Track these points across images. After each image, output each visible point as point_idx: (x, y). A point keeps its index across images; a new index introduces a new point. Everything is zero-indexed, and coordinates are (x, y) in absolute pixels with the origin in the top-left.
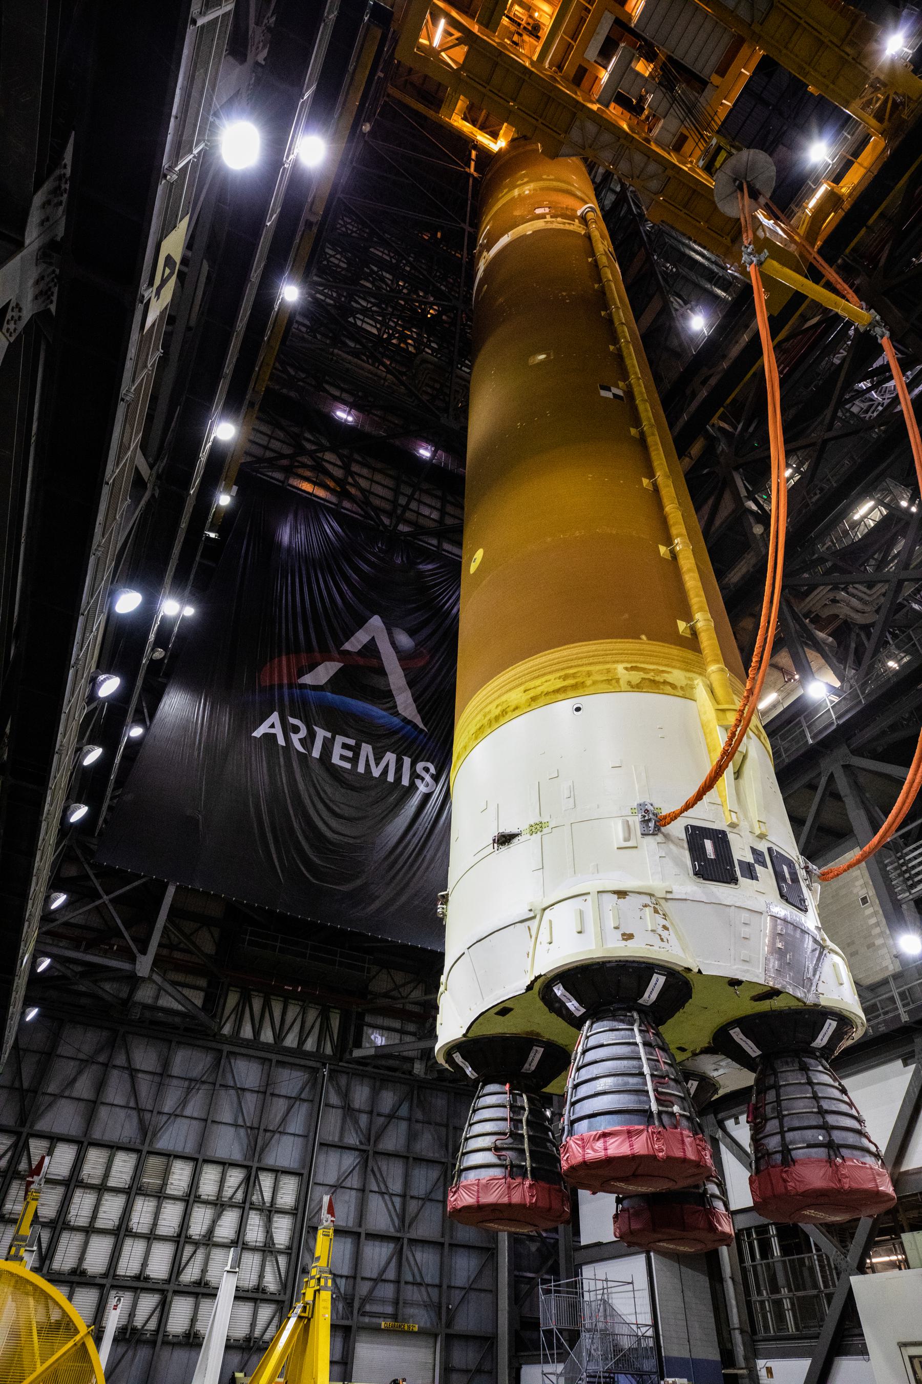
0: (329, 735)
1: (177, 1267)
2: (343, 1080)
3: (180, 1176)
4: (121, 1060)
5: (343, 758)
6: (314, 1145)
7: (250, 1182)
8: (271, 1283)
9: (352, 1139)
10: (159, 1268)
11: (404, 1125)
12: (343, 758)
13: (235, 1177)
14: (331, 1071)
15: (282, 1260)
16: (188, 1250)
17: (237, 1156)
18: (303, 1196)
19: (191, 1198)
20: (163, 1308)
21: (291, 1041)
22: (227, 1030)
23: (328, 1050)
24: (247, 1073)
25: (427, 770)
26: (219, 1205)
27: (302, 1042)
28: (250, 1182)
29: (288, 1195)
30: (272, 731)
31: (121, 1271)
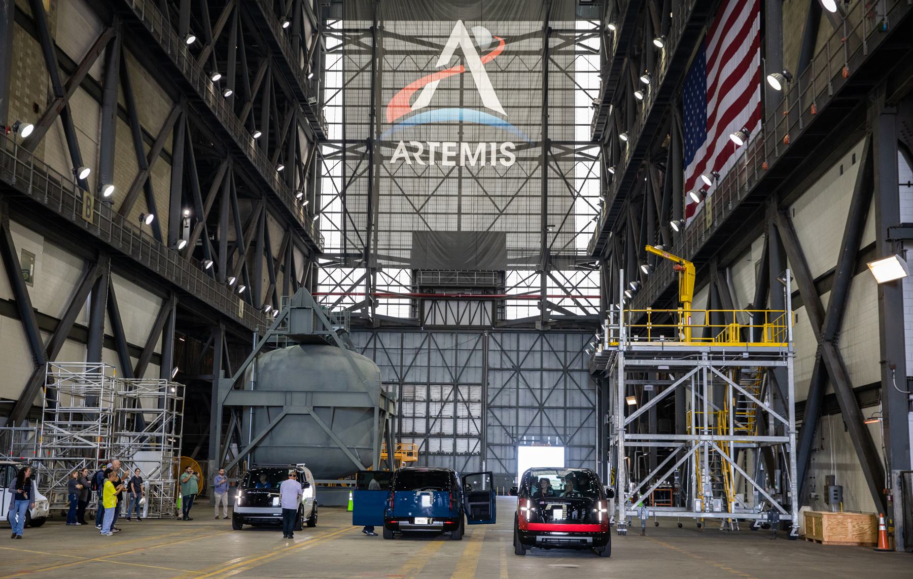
0: (438, 144)
1: (428, 429)
2: (498, 337)
3: (421, 393)
4: (379, 346)
5: (450, 159)
6: (486, 369)
7: (456, 389)
8: (474, 431)
9: (509, 365)
10: (421, 427)
11: (538, 355)
12: (450, 159)
13: (448, 390)
14: (489, 333)
15: (478, 422)
16: (431, 421)
17: (448, 379)
18: (484, 394)
19: (428, 401)
20: (427, 443)
21: (465, 322)
22: (429, 322)
23: (487, 323)
24: (444, 341)
25: (508, 149)
26: (443, 402)
27: (470, 323)
28: (456, 389)
29: (476, 393)
30: (401, 155)
31: (404, 431)
